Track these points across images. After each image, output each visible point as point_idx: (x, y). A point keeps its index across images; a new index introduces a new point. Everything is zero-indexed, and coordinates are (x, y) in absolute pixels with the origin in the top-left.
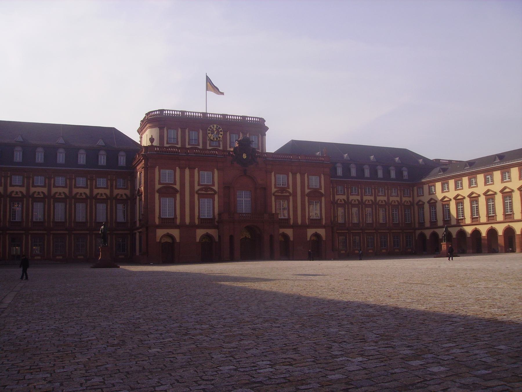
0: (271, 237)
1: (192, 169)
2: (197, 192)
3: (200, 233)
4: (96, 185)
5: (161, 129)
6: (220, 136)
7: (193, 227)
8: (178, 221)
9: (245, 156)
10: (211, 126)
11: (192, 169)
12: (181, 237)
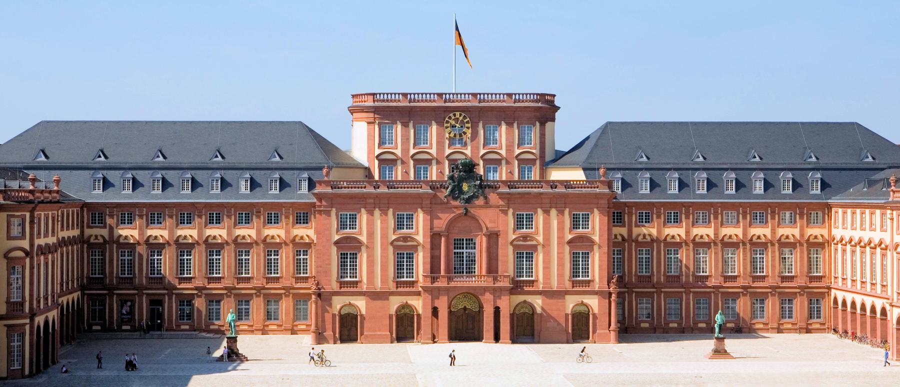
0: (497, 311)
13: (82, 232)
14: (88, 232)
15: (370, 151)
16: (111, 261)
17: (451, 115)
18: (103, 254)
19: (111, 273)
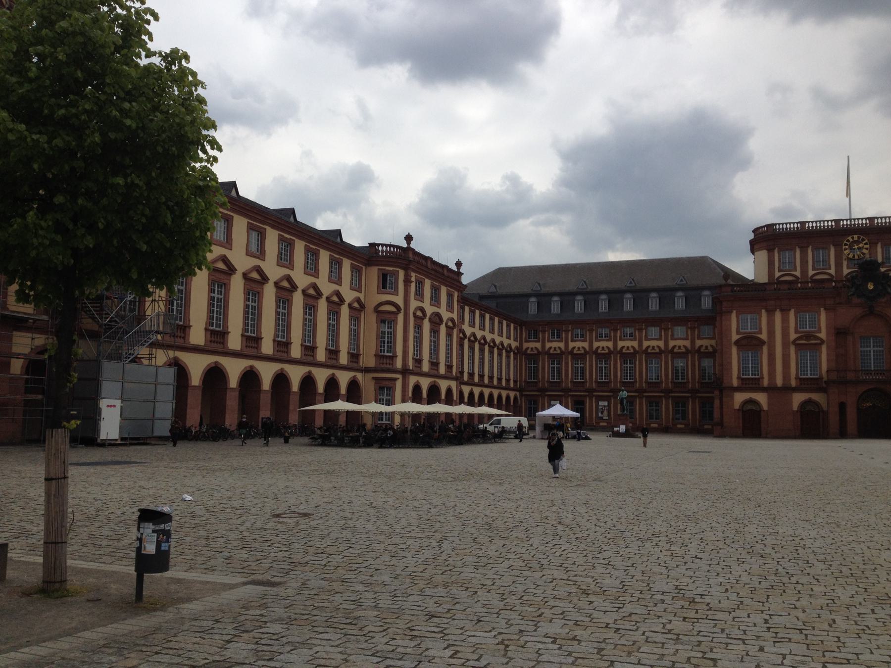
1: (785, 311)
2: (794, 342)
3: (798, 399)
4: (672, 335)
5: (770, 251)
6: (865, 251)
7: (787, 389)
8: (766, 382)
9: (871, 286)
10: (850, 238)
11: (785, 311)
12: (769, 404)
13: (521, 344)
14: (525, 345)
15: (771, 273)
16: (543, 368)
17: (850, 238)
18: (536, 362)
19: (543, 377)
